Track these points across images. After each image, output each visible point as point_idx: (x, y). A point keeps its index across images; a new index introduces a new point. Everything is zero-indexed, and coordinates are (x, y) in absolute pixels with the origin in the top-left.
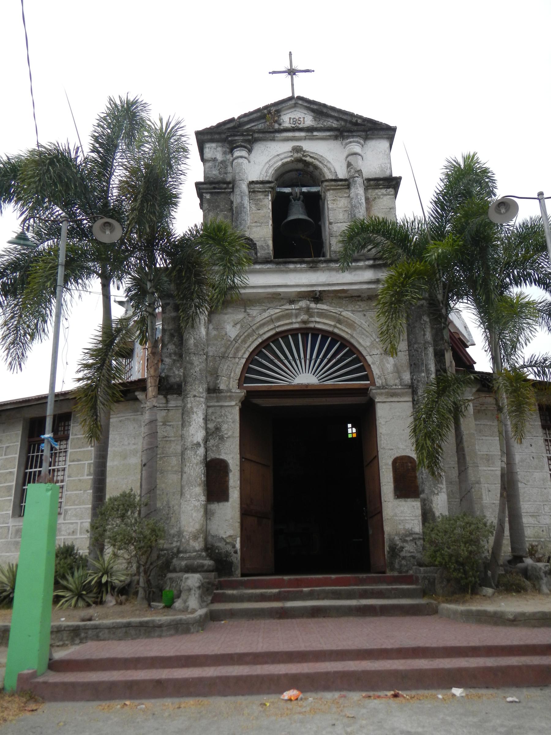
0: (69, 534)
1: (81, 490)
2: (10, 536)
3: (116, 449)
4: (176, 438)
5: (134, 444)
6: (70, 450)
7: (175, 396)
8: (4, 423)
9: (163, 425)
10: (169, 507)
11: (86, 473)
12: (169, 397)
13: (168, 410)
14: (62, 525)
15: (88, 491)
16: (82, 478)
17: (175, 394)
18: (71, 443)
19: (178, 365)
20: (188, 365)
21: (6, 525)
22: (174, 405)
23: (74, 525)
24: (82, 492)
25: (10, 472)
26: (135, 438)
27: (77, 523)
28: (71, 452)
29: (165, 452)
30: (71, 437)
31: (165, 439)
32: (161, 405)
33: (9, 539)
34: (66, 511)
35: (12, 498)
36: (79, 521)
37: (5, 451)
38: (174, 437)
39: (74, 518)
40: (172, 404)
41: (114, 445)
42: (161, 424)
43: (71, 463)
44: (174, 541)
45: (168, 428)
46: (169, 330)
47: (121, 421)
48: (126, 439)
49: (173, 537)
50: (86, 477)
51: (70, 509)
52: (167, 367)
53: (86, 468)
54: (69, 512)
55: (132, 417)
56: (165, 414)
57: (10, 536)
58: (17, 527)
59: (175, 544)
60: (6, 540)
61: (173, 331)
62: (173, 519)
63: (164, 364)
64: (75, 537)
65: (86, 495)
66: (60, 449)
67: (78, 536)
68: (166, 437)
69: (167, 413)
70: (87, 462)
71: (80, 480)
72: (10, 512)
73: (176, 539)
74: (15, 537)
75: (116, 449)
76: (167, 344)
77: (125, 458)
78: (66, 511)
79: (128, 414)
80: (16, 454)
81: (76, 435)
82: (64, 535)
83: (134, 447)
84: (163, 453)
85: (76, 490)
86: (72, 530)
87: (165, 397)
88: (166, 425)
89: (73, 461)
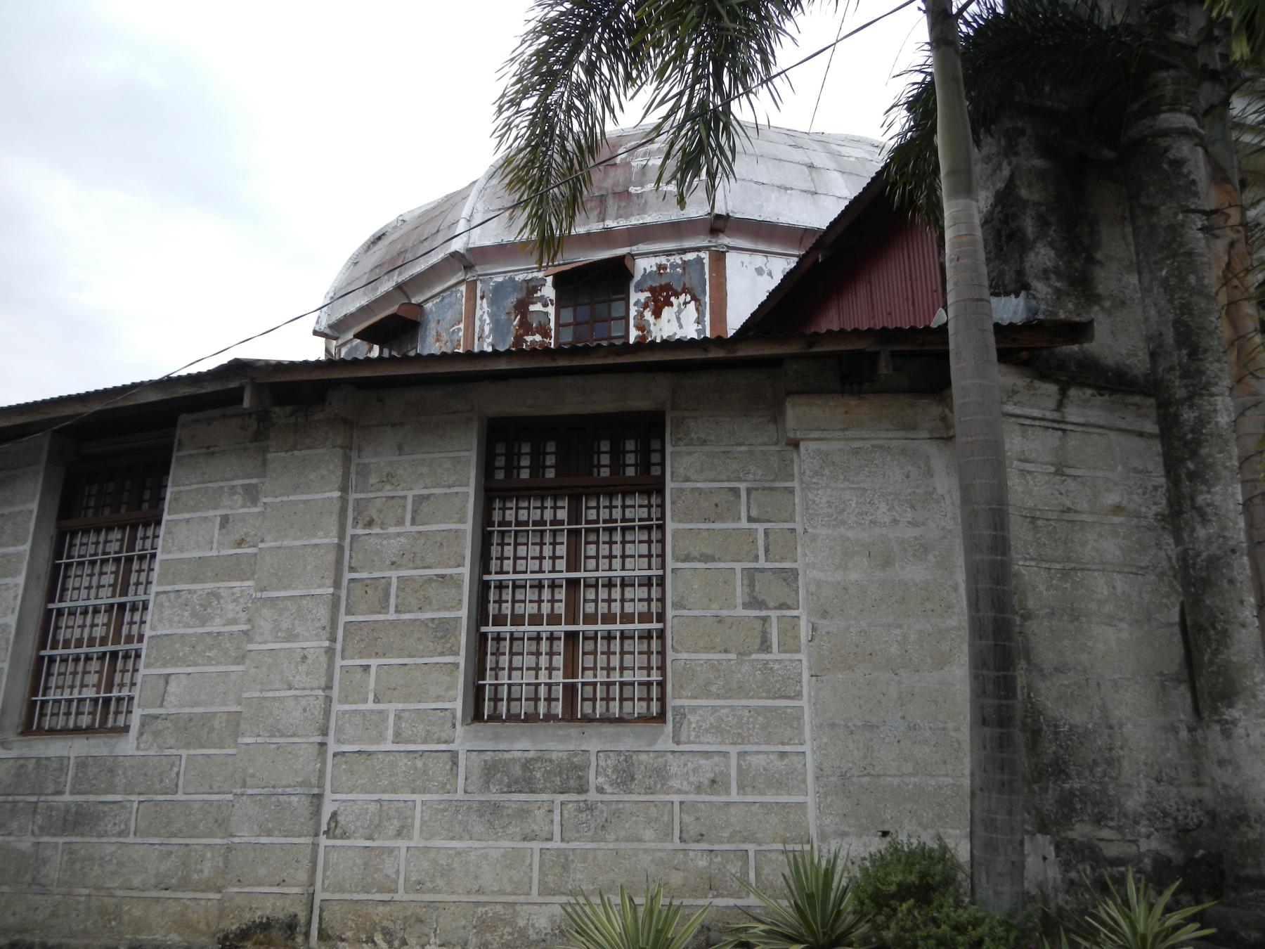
0: (699, 789)
1: (726, 651)
2: (461, 782)
3: (850, 534)
4: (1095, 518)
5: (914, 524)
6: (670, 526)
7: (1089, 392)
8: (402, 424)
9: (1056, 473)
10: (1110, 727)
11: (739, 601)
12: (1073, 392)
13: (1064, 431)
14: (670, 756)
15: (754, 656)
16: (725, 613)
17: (1089, 386)
18: (673, 503)
19: (1070, 306)
20: (1195, 299)
21: (443, 747)
22: (1082, 420)
23: (716, 759)
24: (732, 656)
25: (443, 576)
26: (913, 507)
27: (726, 754)
28: (675, 532)
29: (1073, 556)
30: (669, 485)
31: (1066, 516)
32: (1049, 415)
33: (460, 795)
34: (681, 713)
35: (461, 660)
36: (733, 750)
37: (414, 512)
38: (1091, 513)
39: (709, 738)
40: (1074, 414)
41: (843, 523)
42: (1052, 469)
43: (680, 565)
44: (1139, 835)
45: (1071, 484)
46: (1034, 204)
47: (856, 452)
48: (883, 508)
49: (1137, 823)
50: (740, 612)
51: (694, 709)
52: (1043, 307)
53: (739, 583)
54: (693, 718)
55: (896, 443)
56: (1057, 443)
57: (461, 782)
58: (488, 756)
59: (1144, 846)
60: (446, 796)
61: (1043, 208)
62: (1125, 764)
63: (1035, 298)
64: (723, 799)
65: (746, 667)
66: (518, 523)
67: (734, 796)
68: (1069, 510)
69: (1060, 439)
70: (738, 566)
71: (720, 620)
72: (458, 705)
73: (1143, 830)
74: (486, 787)
75: (850, 534)
76: (1035, 242)
77: (887, 563)
78: (681, 713)
79: (884, 434)
80: (462, 520)
81: (688, 480)
82: (679, 791)
83: (911, 533)
84: (1069, 560)
85: (707, 650)
86: (711, 776)
87: (1063, 393)
88: (1062, 475)
89: (687, 558)
